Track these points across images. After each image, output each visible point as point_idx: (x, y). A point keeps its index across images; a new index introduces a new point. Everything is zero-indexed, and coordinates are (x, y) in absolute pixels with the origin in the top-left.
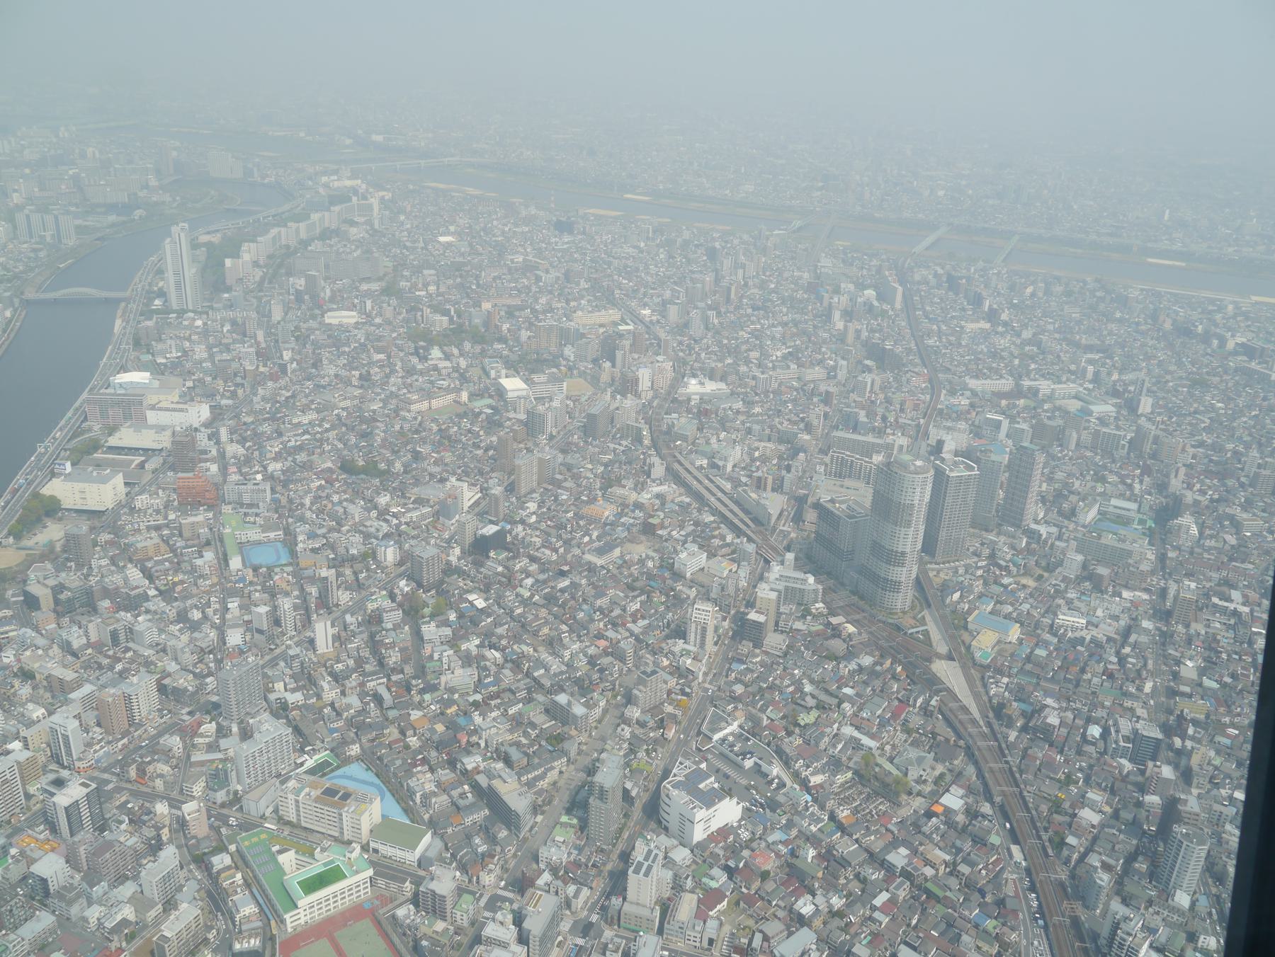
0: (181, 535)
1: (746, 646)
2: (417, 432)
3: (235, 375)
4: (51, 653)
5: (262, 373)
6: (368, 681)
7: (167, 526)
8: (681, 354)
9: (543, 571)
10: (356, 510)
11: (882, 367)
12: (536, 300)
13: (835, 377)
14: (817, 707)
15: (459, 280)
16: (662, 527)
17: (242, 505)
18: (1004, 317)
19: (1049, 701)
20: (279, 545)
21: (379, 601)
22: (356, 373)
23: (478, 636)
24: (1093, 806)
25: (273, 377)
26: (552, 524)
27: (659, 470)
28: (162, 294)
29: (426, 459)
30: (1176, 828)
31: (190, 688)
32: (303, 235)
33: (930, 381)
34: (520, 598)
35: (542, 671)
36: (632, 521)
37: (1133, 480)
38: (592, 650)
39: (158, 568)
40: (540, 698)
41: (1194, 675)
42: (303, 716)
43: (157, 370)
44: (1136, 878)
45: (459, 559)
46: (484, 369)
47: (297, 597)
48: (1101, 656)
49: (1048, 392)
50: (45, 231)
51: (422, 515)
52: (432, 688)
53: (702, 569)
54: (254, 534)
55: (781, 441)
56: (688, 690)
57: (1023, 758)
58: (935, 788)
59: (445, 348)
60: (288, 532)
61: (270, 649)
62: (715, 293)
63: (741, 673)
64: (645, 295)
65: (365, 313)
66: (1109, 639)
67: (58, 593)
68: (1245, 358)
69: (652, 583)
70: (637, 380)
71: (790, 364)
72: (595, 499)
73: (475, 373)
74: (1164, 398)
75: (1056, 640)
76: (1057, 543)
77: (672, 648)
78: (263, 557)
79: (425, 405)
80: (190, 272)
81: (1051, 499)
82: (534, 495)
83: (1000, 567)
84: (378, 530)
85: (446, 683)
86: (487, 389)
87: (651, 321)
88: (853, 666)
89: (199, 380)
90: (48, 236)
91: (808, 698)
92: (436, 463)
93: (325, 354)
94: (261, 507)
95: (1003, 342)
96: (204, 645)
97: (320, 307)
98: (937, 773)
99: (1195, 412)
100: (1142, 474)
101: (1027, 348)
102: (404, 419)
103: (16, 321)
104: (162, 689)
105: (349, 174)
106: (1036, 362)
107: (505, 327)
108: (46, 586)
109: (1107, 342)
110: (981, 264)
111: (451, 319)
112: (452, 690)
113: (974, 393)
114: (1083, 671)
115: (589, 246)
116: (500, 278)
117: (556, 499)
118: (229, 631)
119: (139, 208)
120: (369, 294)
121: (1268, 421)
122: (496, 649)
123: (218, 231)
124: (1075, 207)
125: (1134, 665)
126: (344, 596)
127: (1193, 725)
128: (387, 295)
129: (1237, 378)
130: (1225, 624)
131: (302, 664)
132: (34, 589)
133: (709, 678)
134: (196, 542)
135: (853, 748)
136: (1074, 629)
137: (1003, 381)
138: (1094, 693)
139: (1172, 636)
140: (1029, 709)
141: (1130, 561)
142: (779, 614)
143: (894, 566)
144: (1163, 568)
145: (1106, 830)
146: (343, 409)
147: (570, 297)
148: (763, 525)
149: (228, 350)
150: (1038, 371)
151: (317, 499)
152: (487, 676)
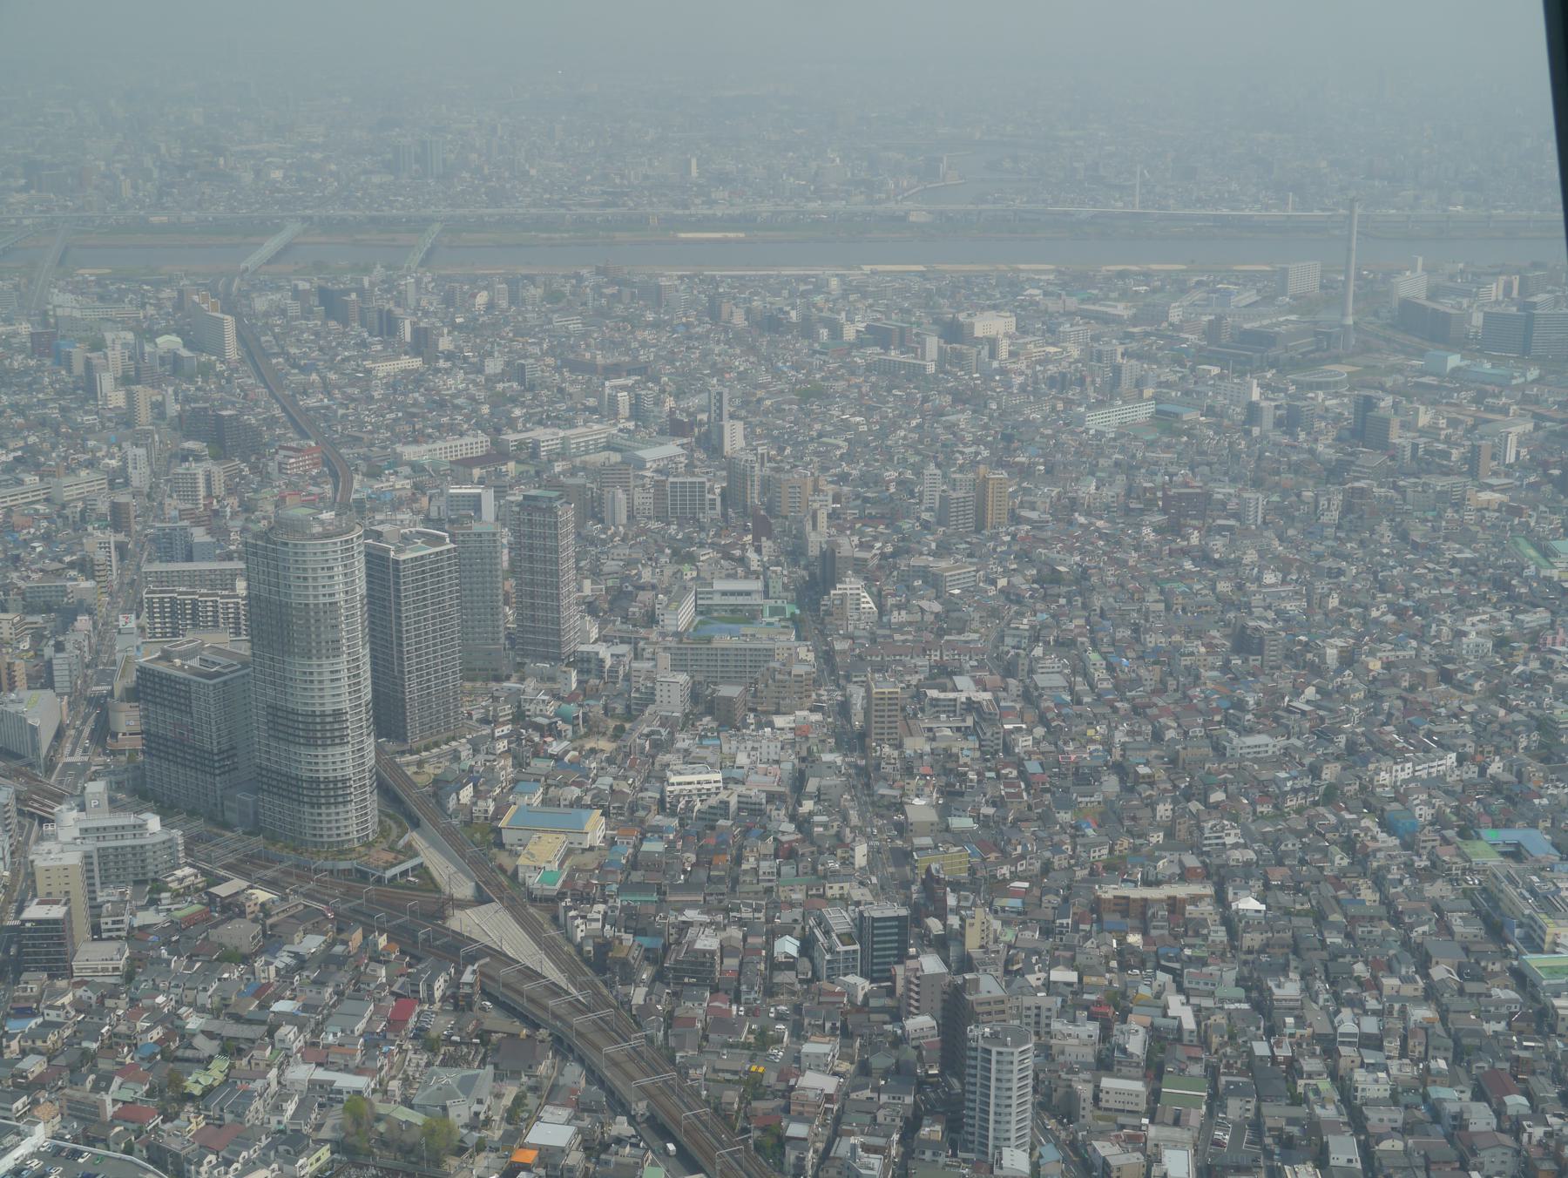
1: (33, 983)
11: (220, 452)
13: (127, 483)
14: (224, 1052)
18: (445, 344)
19: (691, 915)
24: (820, 1065)
30: (973, 1031)
33: (326, 462)
37: (743, 548)
41: (932, 816)
44: (928, 1155)
48: (764, 827)
49: (555, 445)
55: (30, 609)
57: (669, 1027)
58: (511, 1128)
63: (32, 1035)
66: (772, 797)
68: (878, 349)
71: (21, 476)
74: (761, 424)
75: (675, 822)
76: (636, 665)
81: (606, 606)
83: (538, 727)
88: (283, 960)
91: (200, 1041)
95: (454, 383)
98: (507, 1101)
99: (820, 435)
100: (756, 539)
101: (500, 387)
106: (523, 405)
109: (642, 358)
110: (379, 272)
113: (417, 468)
114: (738, 860)
121: (939, 431)
124: (533, 172)
125: (825, 826)
127: (953, 891)
129: (873, 379)
130: (958, 729)
135: (321, 1106)
136: (704, 795)
137: (467, 440)
138: (769, 890)
139: (878, 767)
140: (658, 943)
141: (776, 665)
142: (95, 909)
143: (324, 746)
144: (833, 672)
145: (853, 1096)
148: (18, 756)
150: (528, 418)
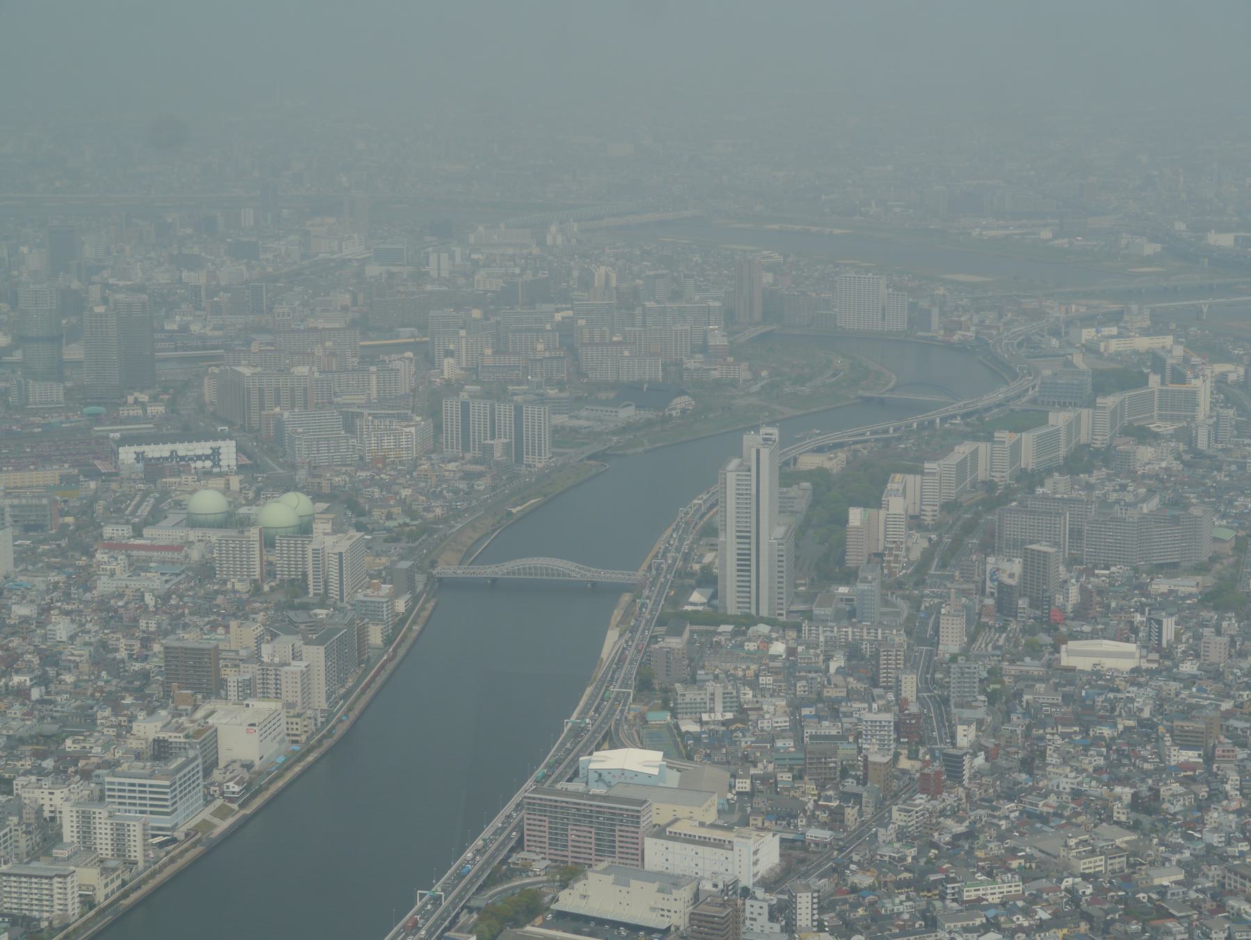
3: (845, 773)
5: (904, 772)
22: (1126, 792)
25: (930, 786)
28: (708, 579)
32: (1028, 460)
50: (493, 437)
65: (1158, 649)
89: (764, 779)
90: (499, 443)
93: (1054, 740)
97: (1051, 628)
103: (414, 622)
119: (682, 393)
120: (1170, 602)
123: (840, 446)
128: (1216, 608)
146: (1085, 877)
149: (835, 715)
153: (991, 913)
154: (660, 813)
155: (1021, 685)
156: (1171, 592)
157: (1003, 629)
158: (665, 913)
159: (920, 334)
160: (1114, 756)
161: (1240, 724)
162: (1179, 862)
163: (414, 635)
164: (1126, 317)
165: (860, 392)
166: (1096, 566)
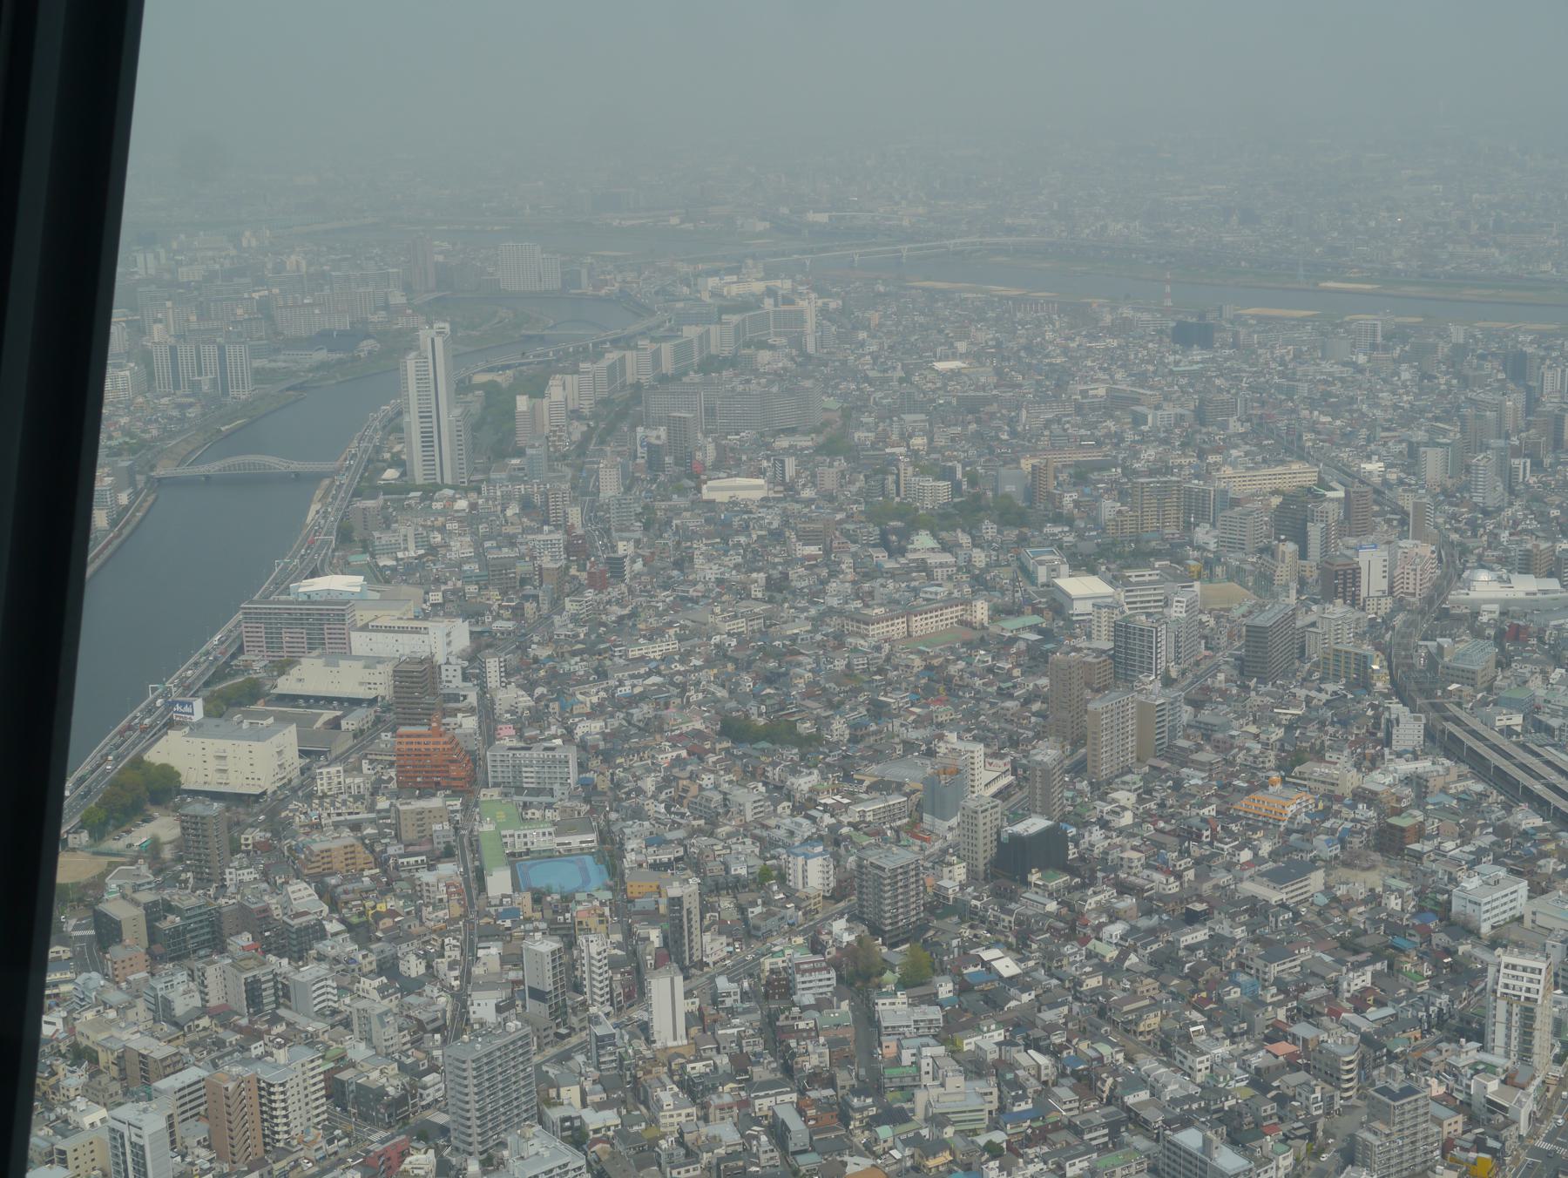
0: (398, 837)
2: (880, 671)
3: (523, 582)
4: (131, 1014)
5: (575, 578)
6: (757, 1097)
7: (372, 822)
8: (1455, 537)
9: (1148, 913)
10: (749, 798)
12: (1135, 455)
15: (973, 427)
16: (1420, 833)
17: (520, 790)
20: (589, 859)
21: (787, 952)
23: (1001, 1024)
25: (597, 582)
26: (1168, 828)
27: (1410, 730)
28: (397, 462)
29: (898, 716)
31: (391, 1090)
32: (668, 366)
34: (1095, 961)
35: (1144, 1095)
36: (1349, 825)
38: (1256, 1060)
39: (349, 887)
40: (1141, 1142)
42: (614, 1156)
43: (376, 576)
45: (962, 887)
46: (1023, 569)
47: (618, 946)
50: (200, 374)
51: (889, 809)
52: (897, 1117)
53: (1520, 919)
54: (539, 838)
56: (1491, 1143)
59: (943, 534)
60: (604, 837)
61: (557, 1035)
62: (1529, 426)
64: (1369, 440)
65: (783, 483)
67: (158, 919)
69: (1399, 941)
70: (1356, 572)
72: (1265, 786)
73: (1004, 576)
77: (1453, 1060)
78: (556, 878)
79: (898, 628)
80: (449, 416)
82: (1127, 778)
84: (791, 833)
85: (929, 1105)
86: (1028, 601)
87: (1385, 482)
89: (454, 592)
92: (919, 722)
93: (700, 547)
94: (558, 793)
96: (424, 1017)
97: (690, 477)
102: (855, 650)
103: (137, 510)
104: (335, 1091)
105: (762, 274)
107: (1068, 499)
108: (136, 903)
111: (956, 488)
112: (938, 1121)
115: (1245, 366)
116: (1059, 422)
117: (1178, 785)
118: (475, 995)
119: (368, 336)
120: (792, 451)
122: (1039, 1049)
126: (716, 945)
131: (621, 1059)
132: (114, 907)
133: (1546, 1128)
134: (427, 847)
146: (729, 634)
147: (1205, 446)
149: (511, 542)
151: (668, 781)
152: (1017, 1099)
153: (653, 665)
154: (363, 616)
155: (669, 514)
156: (791, 446)
157: (653, 480)
158: (372, 686)
159: (572, 291)
160: (749, 556)
161: (850, 527)
162: (807, 618)
163: (136, 520)
164: (744, 271)
165: (524, 332)
166: (728, 434)
